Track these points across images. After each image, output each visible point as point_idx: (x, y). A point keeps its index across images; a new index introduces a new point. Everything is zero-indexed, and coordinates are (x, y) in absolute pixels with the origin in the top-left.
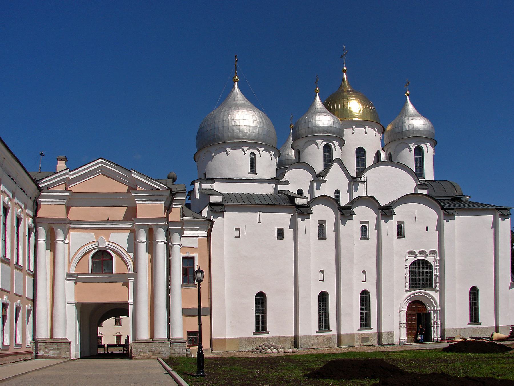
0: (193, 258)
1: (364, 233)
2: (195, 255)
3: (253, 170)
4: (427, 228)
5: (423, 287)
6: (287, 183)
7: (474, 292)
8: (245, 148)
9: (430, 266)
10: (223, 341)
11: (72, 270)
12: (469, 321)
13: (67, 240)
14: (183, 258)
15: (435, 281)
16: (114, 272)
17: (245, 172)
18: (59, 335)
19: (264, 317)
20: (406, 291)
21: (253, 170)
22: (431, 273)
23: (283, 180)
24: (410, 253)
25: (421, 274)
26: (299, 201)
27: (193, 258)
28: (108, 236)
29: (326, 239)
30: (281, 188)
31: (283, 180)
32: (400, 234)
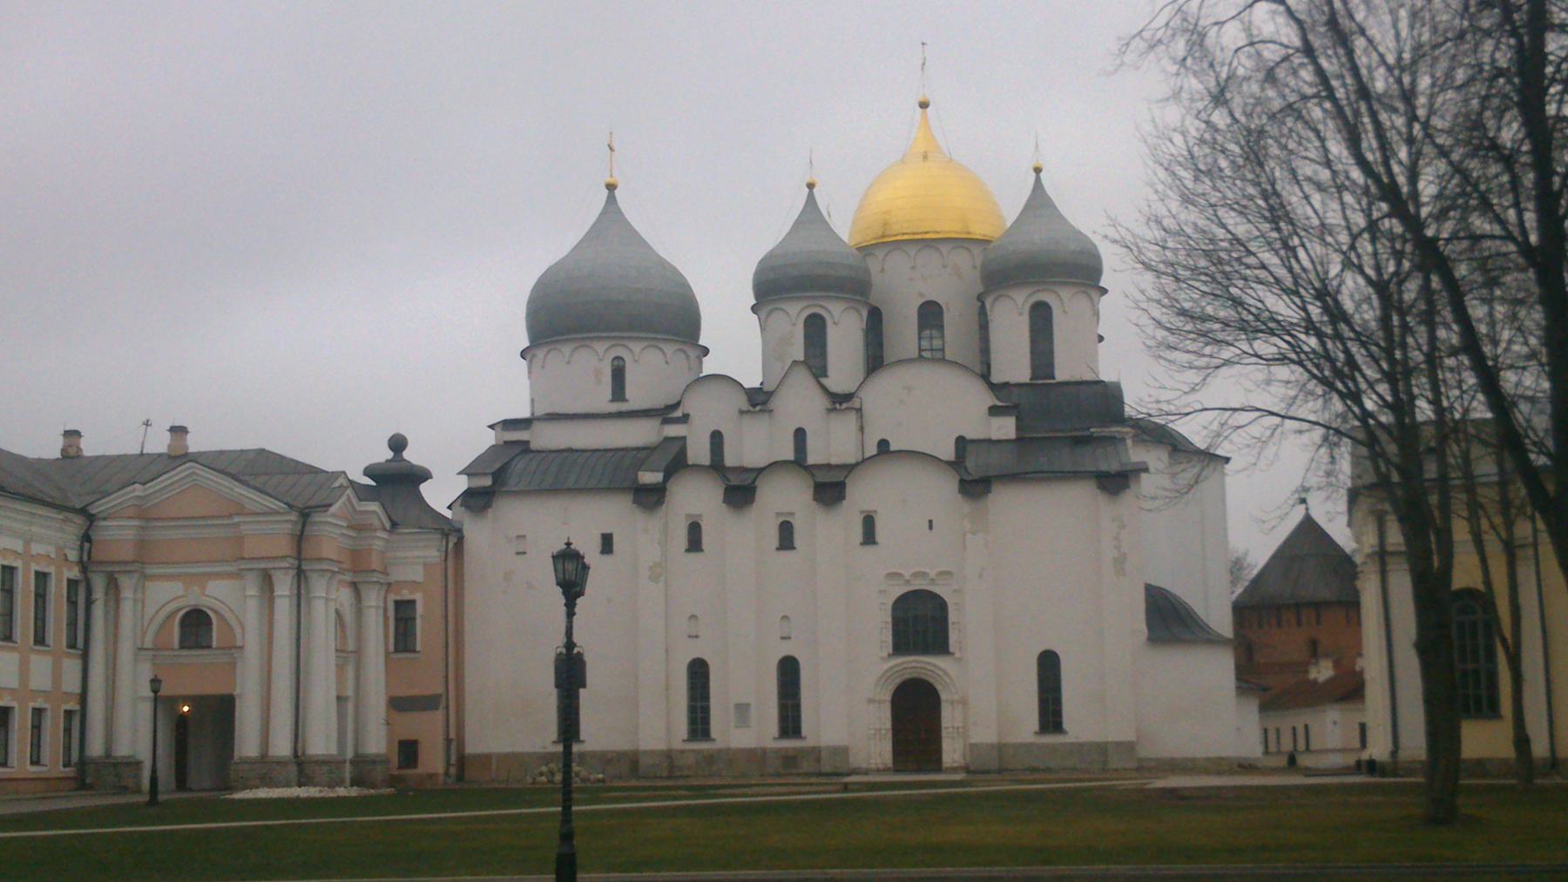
0: (413, 602)
1: (786, 537)
2: (418, 597)
3: (619, 391)
4: (931, 522)
5: (926, 649)
6: (685, 419)
7: (1049, 665)
8: (600, 347)
9: (942, 605)
10: (485, 759)
11: (148, 644)
12: (1036, 727)
13: (140, 596)
14: (398, 604)
15: (953, 637)
16: (214, 644)
17: (601, 399)
18: (123, 750)
19: (706, 711)
20: (883, 659)
21: (619, 391)
22: (945, 619)
23: (678, 413)
24: (893, 575)
25: (921, 622)
26: (649, 477)
27: (413, 602)
28: (203, 587)
29: (688, 551)
30: (673, 431)
31: (678, 413)
32: (869, 537)
